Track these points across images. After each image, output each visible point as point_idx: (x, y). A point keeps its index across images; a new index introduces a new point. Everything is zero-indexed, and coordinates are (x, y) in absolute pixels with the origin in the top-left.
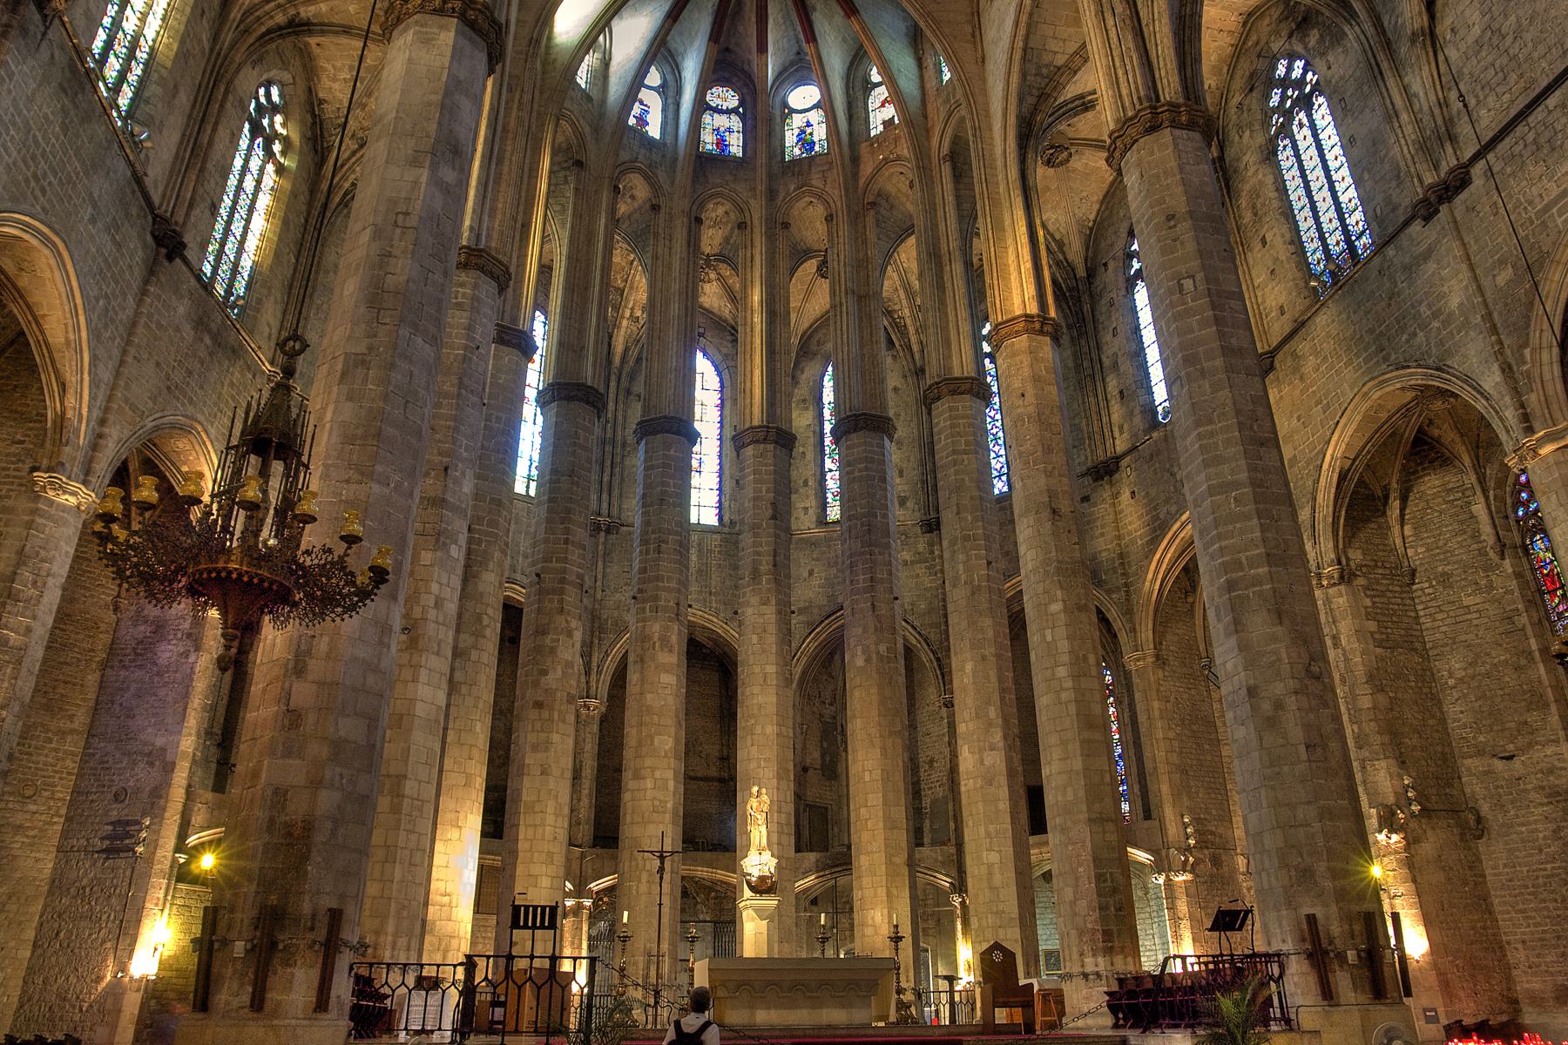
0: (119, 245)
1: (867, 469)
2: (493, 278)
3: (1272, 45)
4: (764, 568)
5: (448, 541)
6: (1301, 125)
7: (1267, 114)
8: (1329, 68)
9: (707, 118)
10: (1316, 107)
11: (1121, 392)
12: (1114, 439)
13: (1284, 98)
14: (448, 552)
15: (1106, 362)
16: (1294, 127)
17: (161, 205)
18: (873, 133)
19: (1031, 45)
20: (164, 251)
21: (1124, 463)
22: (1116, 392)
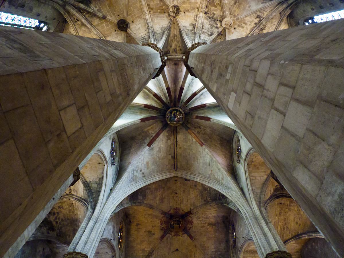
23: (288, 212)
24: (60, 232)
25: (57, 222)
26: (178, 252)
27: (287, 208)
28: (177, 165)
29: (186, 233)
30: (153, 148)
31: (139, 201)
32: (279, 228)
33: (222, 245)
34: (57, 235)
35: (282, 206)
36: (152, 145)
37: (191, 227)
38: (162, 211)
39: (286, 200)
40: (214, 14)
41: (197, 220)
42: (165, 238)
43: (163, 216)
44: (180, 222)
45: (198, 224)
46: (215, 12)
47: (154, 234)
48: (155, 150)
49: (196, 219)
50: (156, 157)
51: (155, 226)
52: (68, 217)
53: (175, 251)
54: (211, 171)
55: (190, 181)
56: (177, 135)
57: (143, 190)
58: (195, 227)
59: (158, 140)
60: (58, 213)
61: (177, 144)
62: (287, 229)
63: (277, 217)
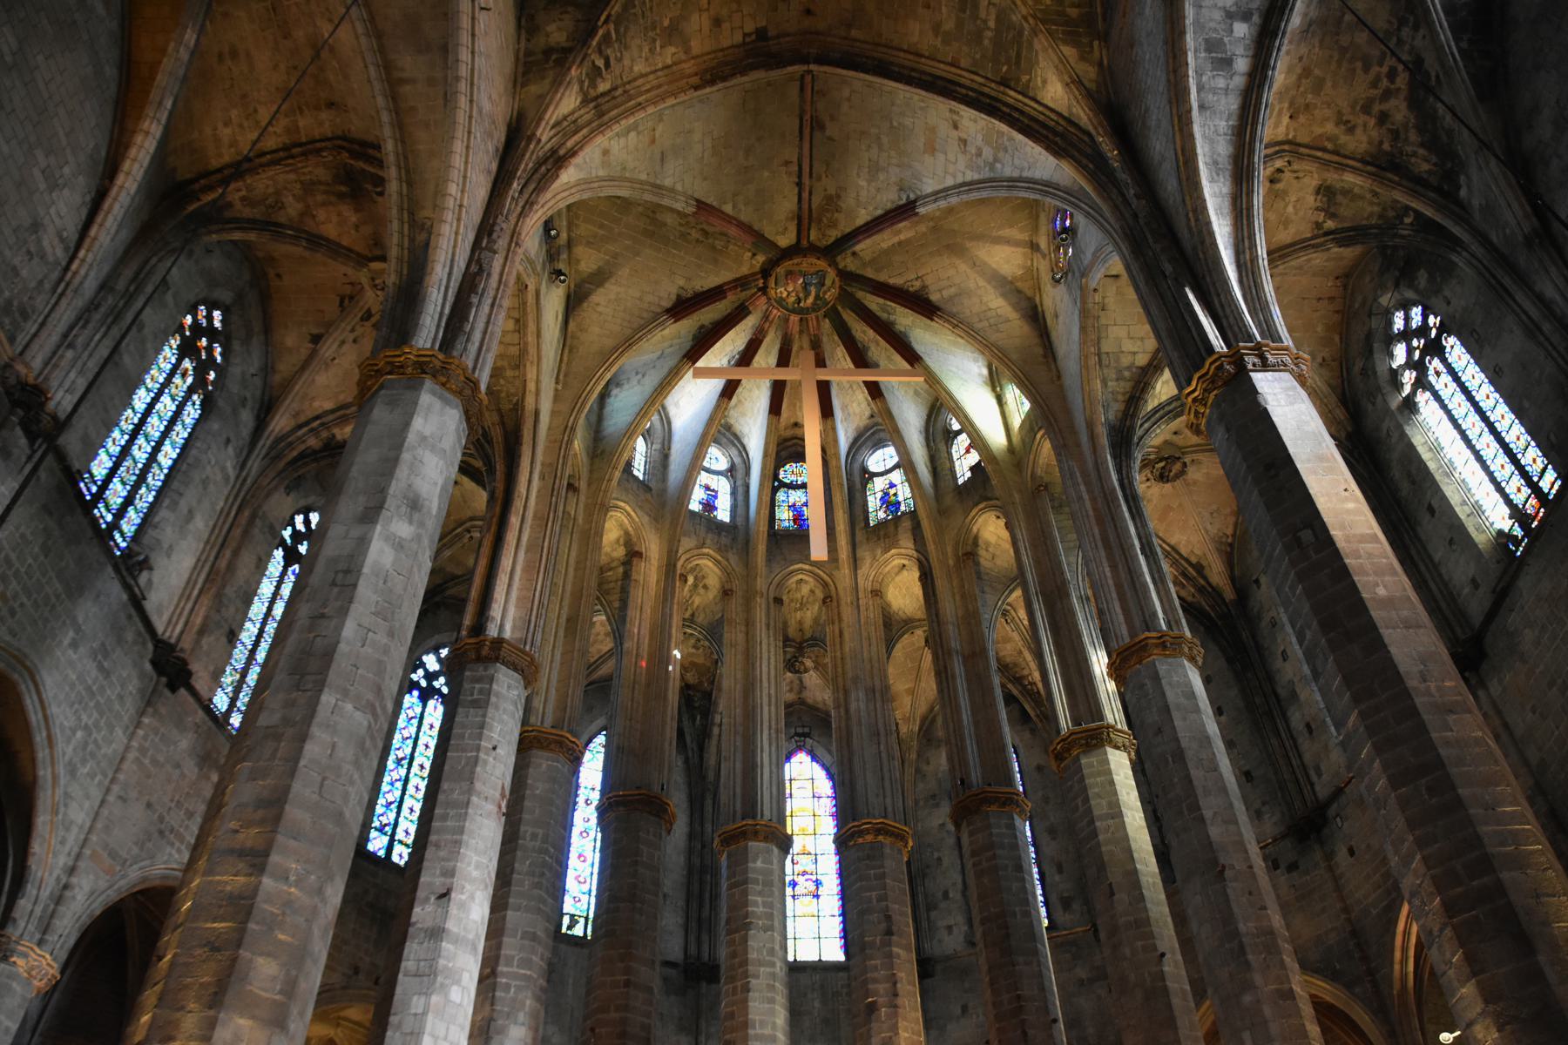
0: (106, 673)
1: (994, 857)
2: (515, 669)
3: (1381, 300)
4: (881, 1000)
5: (447, 982)
6: (1438, 374)
7: (1395, 375)
8: (1449, 303)
9: (781, 495)
10: (1448, 349)
11: (1308, 726)
12: (1312, 785)
13: (1410, 351)
14: (446, 995)
15: (1282, 693)
16: (1430, 378)
17: (165, 631)
18: (961, 481)
19: (1105, 348)
20: (164, 680)
21: (1332, 811)
22: (1301, 727)
24: (1402, 22)
25: (1392, 75)
28: (802, 89)
30: (901, 189)
34: (1416, 28)
36: (901, 203)
40: (695, 647)
46: (694, 651)
48: (893, 179)
50: (893, 153)
52: (1339, 63)
54: (653, 141)
55: (745, 35)
56: (800, 208)
57: (965, 49)
59: (876, 208)
60: (1366, 109)
61: (800, 176)
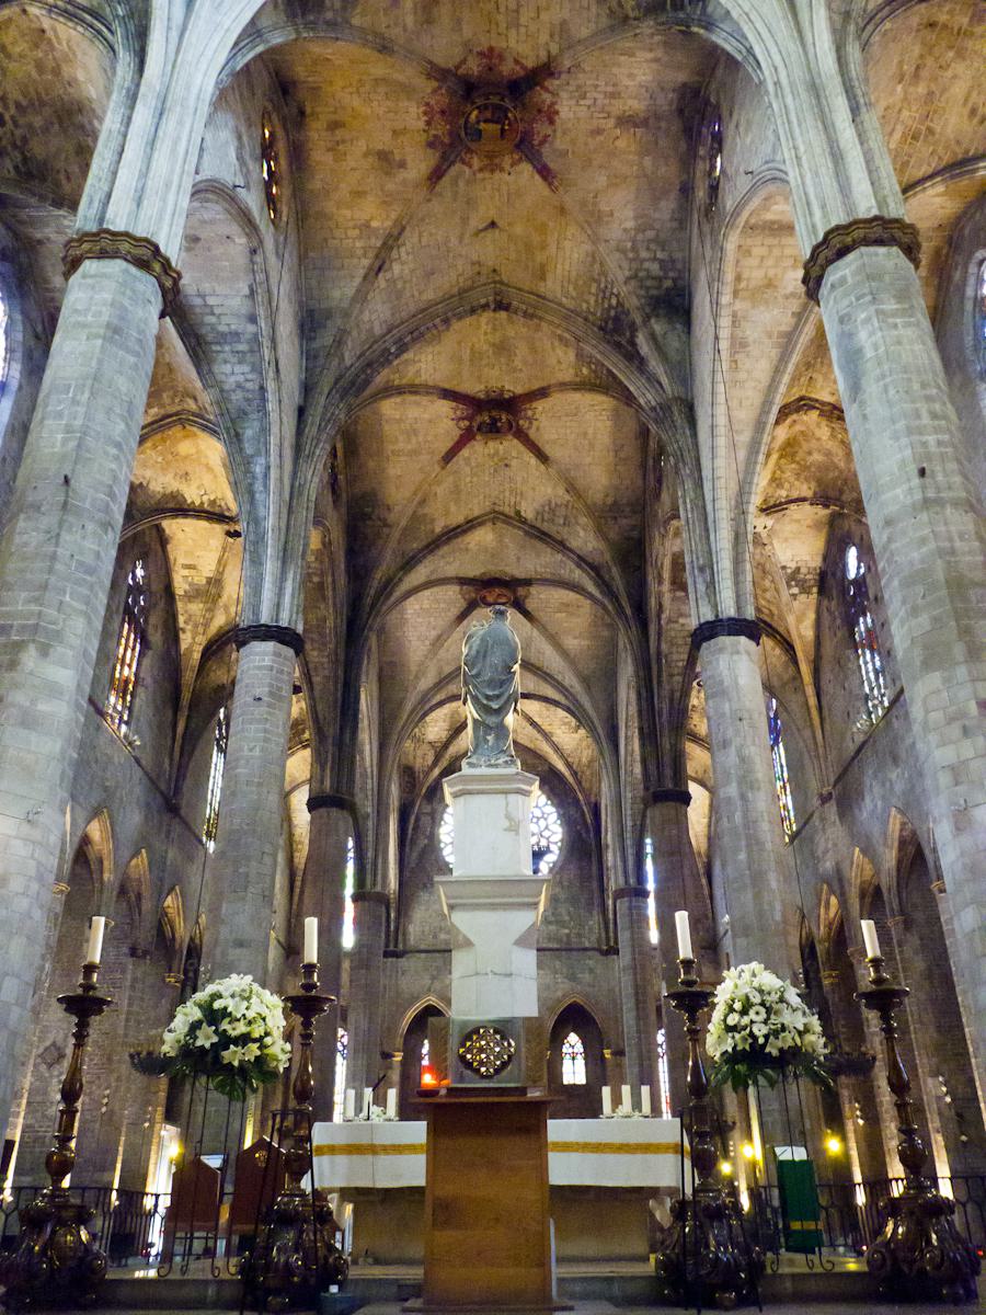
23: (953, 65)
24: (25, 160)
26: (497, 231)
27: (951, 47)
29: (530, 160)
31: (329, 15)
32: (897, 135)
33: (663, 204)
35: (931, 36)
37: (549, 132)
38: (430, 62)
39: (958, 8)
41: (573, 102)
42: (446, 180)
43: (435, 84)
44: (506, 110)
45: (578, 119)
47: (402, 165)
49: (571, 98)
51: (404, 131)
53: (486, 229)
58: (564, 133)
62: (926, 136)
63: (899, 88)
